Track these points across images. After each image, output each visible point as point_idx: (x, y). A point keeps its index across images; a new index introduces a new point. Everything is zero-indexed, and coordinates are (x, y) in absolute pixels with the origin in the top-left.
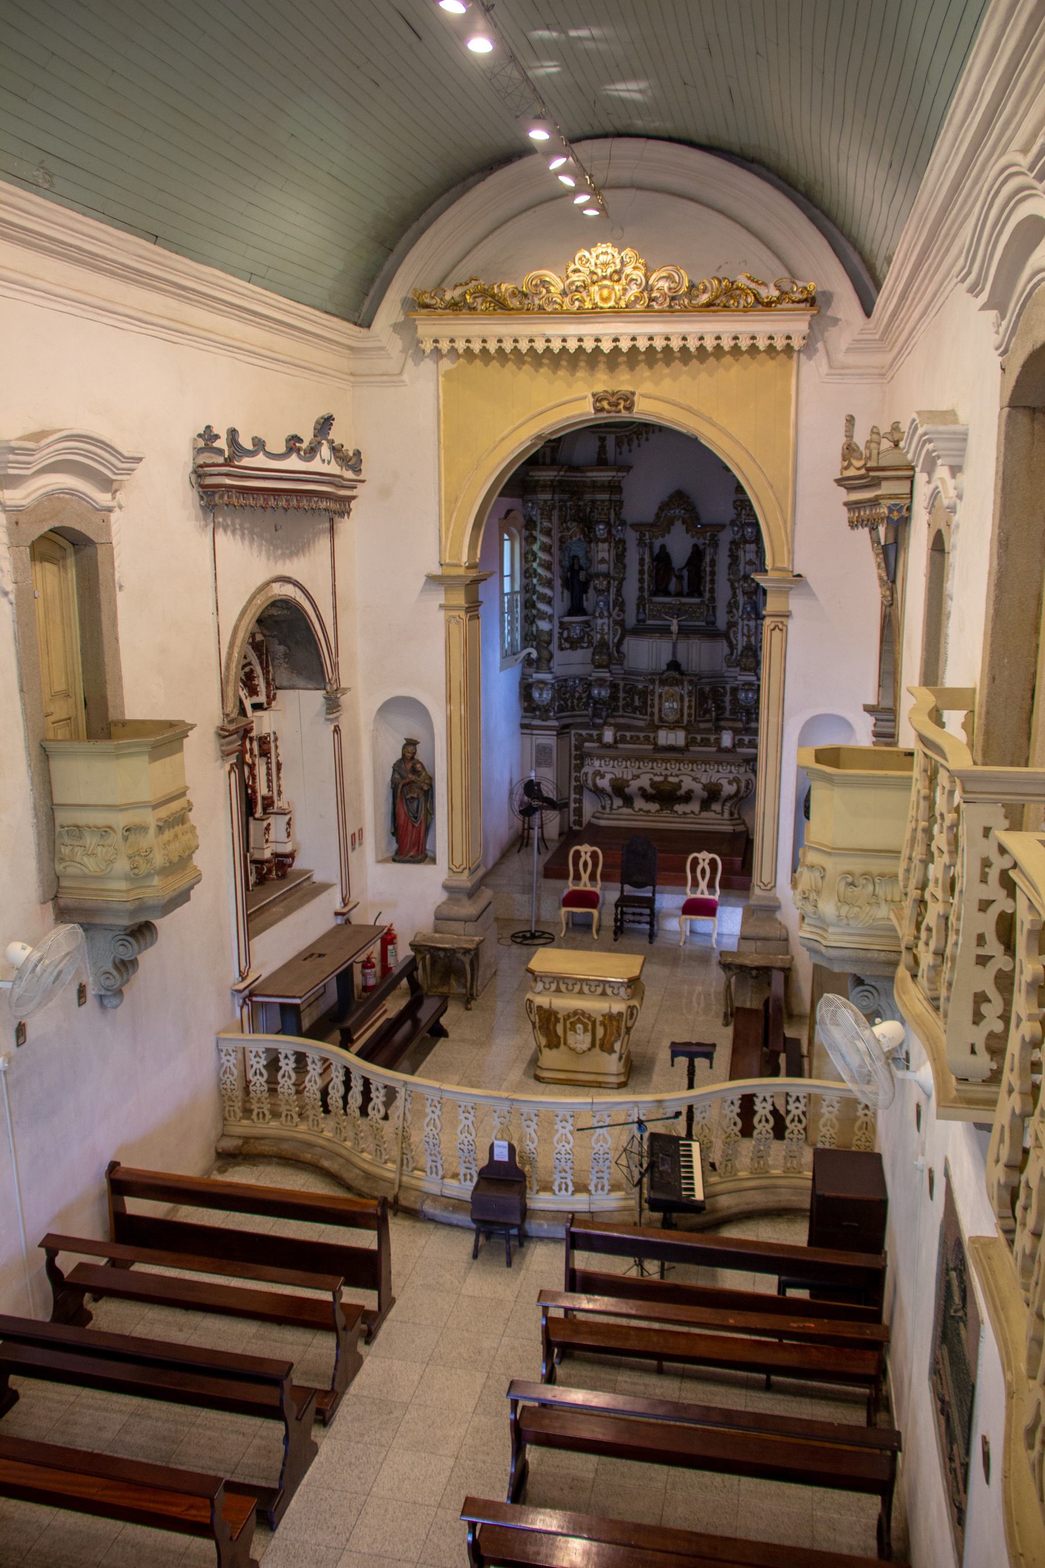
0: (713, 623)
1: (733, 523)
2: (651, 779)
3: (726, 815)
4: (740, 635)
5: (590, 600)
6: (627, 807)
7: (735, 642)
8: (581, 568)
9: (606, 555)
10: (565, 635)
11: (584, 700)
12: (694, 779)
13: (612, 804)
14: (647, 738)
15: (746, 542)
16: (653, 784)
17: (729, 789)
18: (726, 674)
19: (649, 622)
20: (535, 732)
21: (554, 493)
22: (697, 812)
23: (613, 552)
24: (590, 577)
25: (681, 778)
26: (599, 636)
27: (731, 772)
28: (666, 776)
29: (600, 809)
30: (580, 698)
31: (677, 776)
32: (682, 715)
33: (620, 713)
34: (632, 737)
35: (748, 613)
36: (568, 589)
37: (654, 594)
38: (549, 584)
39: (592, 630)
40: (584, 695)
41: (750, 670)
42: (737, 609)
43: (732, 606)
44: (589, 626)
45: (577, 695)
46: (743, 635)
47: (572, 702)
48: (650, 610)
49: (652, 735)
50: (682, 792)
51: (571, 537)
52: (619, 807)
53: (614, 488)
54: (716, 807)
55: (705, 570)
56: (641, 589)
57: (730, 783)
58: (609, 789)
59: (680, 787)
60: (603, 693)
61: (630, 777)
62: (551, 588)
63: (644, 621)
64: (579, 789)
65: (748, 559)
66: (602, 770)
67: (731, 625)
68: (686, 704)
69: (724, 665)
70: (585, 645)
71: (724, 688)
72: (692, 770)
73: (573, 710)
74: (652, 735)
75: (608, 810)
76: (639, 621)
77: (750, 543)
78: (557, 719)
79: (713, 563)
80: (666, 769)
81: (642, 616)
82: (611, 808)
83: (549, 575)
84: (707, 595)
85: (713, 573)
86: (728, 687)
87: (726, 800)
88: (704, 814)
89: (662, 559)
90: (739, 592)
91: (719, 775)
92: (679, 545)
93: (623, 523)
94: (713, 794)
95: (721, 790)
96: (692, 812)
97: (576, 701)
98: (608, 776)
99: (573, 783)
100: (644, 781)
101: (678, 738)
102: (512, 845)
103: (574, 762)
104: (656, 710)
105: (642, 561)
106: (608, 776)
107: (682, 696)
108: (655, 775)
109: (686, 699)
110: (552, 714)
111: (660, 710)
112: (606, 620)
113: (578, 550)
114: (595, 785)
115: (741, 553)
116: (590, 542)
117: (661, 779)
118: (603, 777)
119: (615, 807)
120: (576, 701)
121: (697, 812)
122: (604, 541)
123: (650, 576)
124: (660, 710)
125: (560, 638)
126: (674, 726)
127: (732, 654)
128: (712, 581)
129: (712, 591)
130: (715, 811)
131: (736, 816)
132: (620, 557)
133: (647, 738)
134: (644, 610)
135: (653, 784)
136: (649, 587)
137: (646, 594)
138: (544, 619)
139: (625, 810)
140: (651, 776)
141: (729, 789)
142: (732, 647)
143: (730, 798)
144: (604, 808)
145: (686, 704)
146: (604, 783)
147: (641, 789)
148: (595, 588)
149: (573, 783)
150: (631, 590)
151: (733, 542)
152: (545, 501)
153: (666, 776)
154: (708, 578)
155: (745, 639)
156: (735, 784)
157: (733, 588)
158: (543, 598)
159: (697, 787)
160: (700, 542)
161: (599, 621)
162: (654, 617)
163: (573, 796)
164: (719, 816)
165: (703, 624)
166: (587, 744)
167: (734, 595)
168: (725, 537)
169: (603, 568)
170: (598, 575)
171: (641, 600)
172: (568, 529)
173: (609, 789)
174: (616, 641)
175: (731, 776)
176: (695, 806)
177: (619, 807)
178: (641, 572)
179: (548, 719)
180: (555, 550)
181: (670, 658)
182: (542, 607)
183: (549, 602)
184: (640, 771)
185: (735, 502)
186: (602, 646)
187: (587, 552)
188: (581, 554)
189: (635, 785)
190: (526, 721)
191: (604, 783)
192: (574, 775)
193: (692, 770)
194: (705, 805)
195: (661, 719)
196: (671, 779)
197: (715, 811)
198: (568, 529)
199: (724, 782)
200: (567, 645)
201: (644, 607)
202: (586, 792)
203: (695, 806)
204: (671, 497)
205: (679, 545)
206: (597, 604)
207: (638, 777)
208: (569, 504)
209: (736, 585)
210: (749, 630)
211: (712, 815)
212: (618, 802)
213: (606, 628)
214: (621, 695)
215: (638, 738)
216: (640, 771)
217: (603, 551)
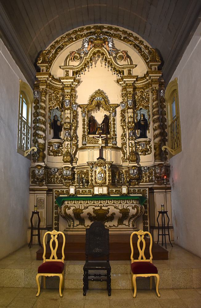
0: (116, 144)
1: (122, 103)
2: (93, 209)
3: (131, 226)
4: (127, 149)
5: (62, 134)
6: (81, 225)
7: (126, 151)
8: (58, 120)
9: (69, 116)
10: (51, 149)
11: (59, 179)
12: (115, 207)
13: (74, 224)
14: (90, 191)
15: (129, 108)
16: (95, 211)
17: (133, 211)
18: (123, 165)
19: (87, 145)
20: (36, 192)
21: (47, 87)
22: (116, 226)
23: (72, 115)
24: (62, 125)
25: (109, 207)
26: (66, 149)
27: (133, 203)
28: (101, 207)
29: (68, 227)
30: (58, 178)
31: (107, 206)
32: (106, 180)
33: (76, 184)
34: (82, 191)
35: (132, 136)
36: (52, 128)
37: (89, 133)
38: (44, 123)
39: (63, 148)
40: (60, 177)
41: (134, 161)
42: (126, 138)
43: (124, 136)
44: (62, 146)
45: (56, 176)
46: (129, 147)
47: (54, 180)
48: (88, 140)
49: (92, 190)
50: (109, 214)
51: (54, 107)
52: (77, 225)
53: (73, 90)
54: (126, 222)
55: (110, 123)
56: (84, 132)
57: (133, 208)
58: (72, 215)
59: (109, 212)
60: (68, 173)
61: (83, 208)
62: (45, 125)
63: (86, 145)
64: (57, 219)
65: (129, 116)
66: (69, 205)
67: (124, 144)
68: (107, 175)
69: (121, 162)
70: (60, 155)
71: (122, 171)
72: (114, 203)
73: (55, 183)
74: (92, 190)
75: (72, 227)
76: (83, 144)
77: (130, 109)
78: (47, 186)
79: (114, 120)
80: (101, 203)
81: (84, 143)
82: (73, 226)
83: (44, 119)
84: (112, 133)
85: (114, 124)
86: (124, 171)
87: (131, 218)
88: (120, 226)
89: (92, 122)
90: (126, 130)
91: (127, 205)
92: (99, 116)
93: (76, 104)
94: (125, 214)
95: (129, 212)
96: (114, 226)
97: (55, 179)
98: (72, 208)
99: (54, 215)
100: (90, 210)
101: (104, 190)
102: (23, 247)
103: (54, 205)
104: (93, 178)
105: (84, 121)
106: (72, 208)
107: (105, 171)
108: (96, 206)
109: (107, 173)
110: (44, 183)
111: (95, 178)
112: (69, 143)
113: (58, 113)
114: (65, 213)
115: (126, 115)
116: (62, 111)
117: (99, 208)
118: (69, 208)
119: (75, 225)
120: (55, 179)
121: (116, 226)
122: (68, 109)
123: (87, 126)
124: (95, 178)
125: (49, 150)
126: (101, 185)
127: (124, 156)
128: (114, 128)
129: (114, 131)
130: (125, 224)
131: (135, 227)
132: (75, 117)
133: (90, 191)
134: (86, 140)
135: (95, 211)
136: (87, 130)
137: (86, 134)
138: (41, 138)
139: (80, 226)
140: (94, 207)
141: (133, 211)
142: (124, 154)
143: (133, 216)
144: (70, 226)
145: (107, 175)
146: (70, 212)
147: (89, 214)
148: (65, 129)
149: (54, 215)
150: (80, 132)
151: (122, 111)
152: (43, 89)
153: (101, 207)
154: (112, 126)
155: (130, 149)
156: (135, 209)
157: (124, 129)
158: (41, 129)
159: (117, 211)
160: (108, 114)
161: (66, 143)
162: (90, 143)
163: (54, 222)
164: (128, 227)
165: (111, 145)
166: (61, 196)
167: (124, 131)
168: (119, 110)
169: (68, 120)
170: (65, 123)
171: (84, 136)
172: (53, 103)
173: (72, 215)
174: (73, 152)
175: (133, 205)
176: (115, 223)
177: (77, 225)
178: (84, 124)
179: (43, 185)
180: (47, 110)
181: (98, 156)
182: (40, 133)
183: (44, 131)
184: (88, 205)
185: (122, 94)
186: (68, 153)
187: (60, 115)
188: (59, 116)
189: (86, 211)
190: (31, 187)
191: (70, 212)
192: (55, 211)
193: (114, 203)
194: (120, 222)
195: (96, 182)
196: (103, 208)
197: (125, 224)
198: (53, 103)
199: (130, 208)
200: (52, 154)
201: (85, 138)
202: (61, 219)
203: (115, 223)
204: (96, 93)
205: (99, 116)
206: (65, 134)
207: (87, 208)
208: (53, 95)
209: (125, 127)
210: (132, 145)
211: (124, 226)
212: (77, 222)
213: (69, 146)
214: (76, 176)
215: (86, 191)
216: (88, 205)
217: (68, 114)
